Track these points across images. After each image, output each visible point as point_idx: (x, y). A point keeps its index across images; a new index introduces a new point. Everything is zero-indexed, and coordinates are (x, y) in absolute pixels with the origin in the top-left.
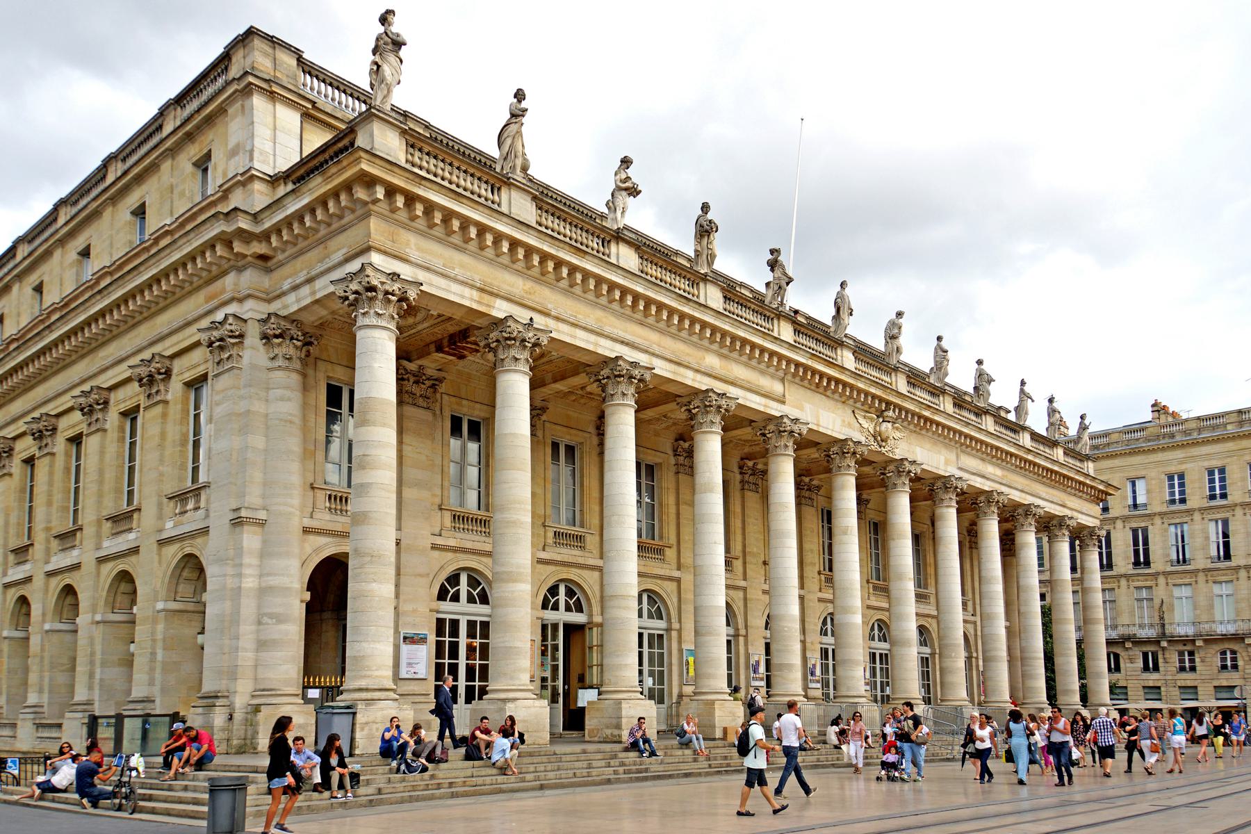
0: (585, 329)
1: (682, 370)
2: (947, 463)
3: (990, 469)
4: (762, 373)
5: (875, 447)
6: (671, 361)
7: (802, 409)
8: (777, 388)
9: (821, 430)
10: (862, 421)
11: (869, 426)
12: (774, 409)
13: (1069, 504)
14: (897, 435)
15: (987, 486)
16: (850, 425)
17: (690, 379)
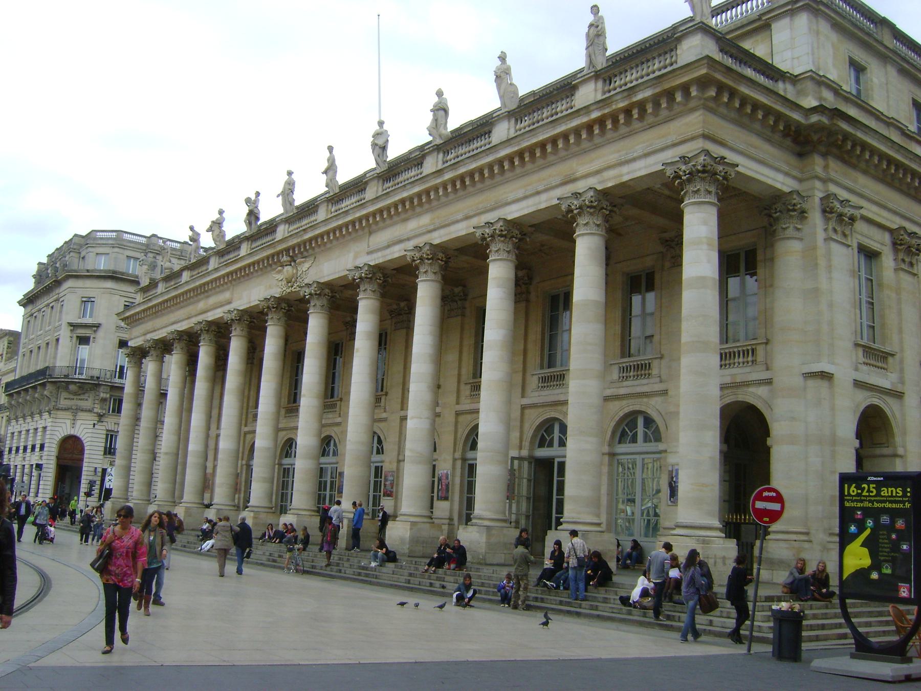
2: (355, 258)
3: (413, 225)
8: (226, 295)
14: (307, 265)
16: (270, 287)
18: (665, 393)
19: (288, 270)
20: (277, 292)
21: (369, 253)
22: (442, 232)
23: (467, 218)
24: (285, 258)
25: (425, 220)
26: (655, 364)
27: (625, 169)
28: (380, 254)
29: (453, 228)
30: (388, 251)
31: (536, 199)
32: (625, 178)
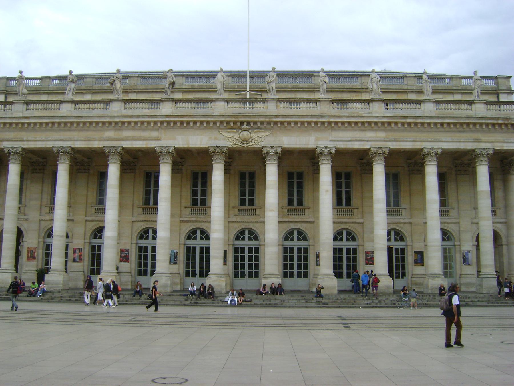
0: (40, 141)
1: (91, 142)
2: (317, 139)
3: (370, 134)
4: (144, 130)
5: (237, 145)
6: (85, 140)
7: (175, 139)
8: (155, 134)
9: (191, 146)
10: (226, 134)
11: (236, 136)
12: (152, 144)
13: (484, 139)
14: (262, 134)
15: (367, 145)
16: (216, 139)
17: (96, 144)
18: (459, 223)
19: (245, 134)
20: (228, 144)
21: (331, 141)
22: (394, 143)
23: (414, 141)
24: (245, 126)
25: (381, 134)
26: (451, 211)
27: (505, 145)
28: (341, 143)
29: (402, 143)
30: (350, 143)
31: (458, 144)
32: (505, 148)
